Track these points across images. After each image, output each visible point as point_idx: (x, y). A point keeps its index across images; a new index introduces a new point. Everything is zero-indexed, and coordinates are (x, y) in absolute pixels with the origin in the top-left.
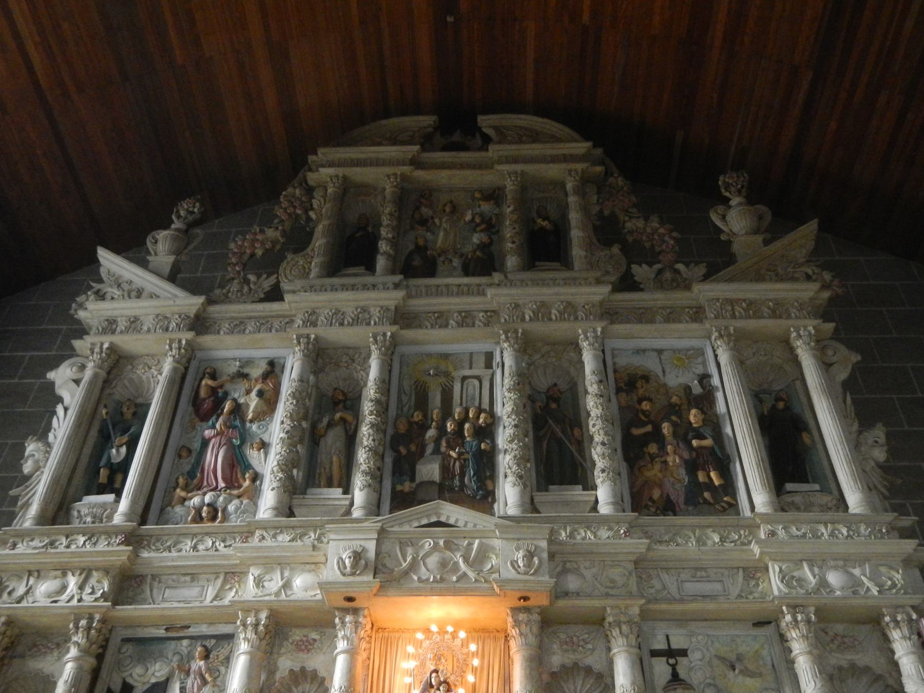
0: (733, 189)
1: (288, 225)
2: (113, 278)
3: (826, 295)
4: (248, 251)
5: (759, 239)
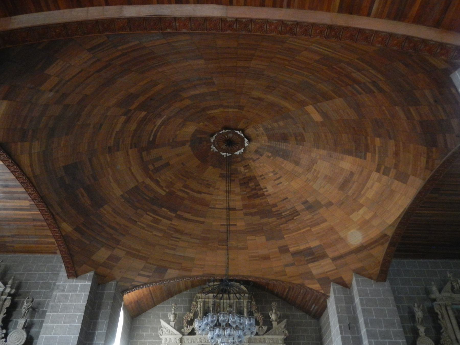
0: (274, 307)
1: (194, 312)
2: (164, 326)
3: (285, 337)
4: (187, 319)
5: (276, 322)
